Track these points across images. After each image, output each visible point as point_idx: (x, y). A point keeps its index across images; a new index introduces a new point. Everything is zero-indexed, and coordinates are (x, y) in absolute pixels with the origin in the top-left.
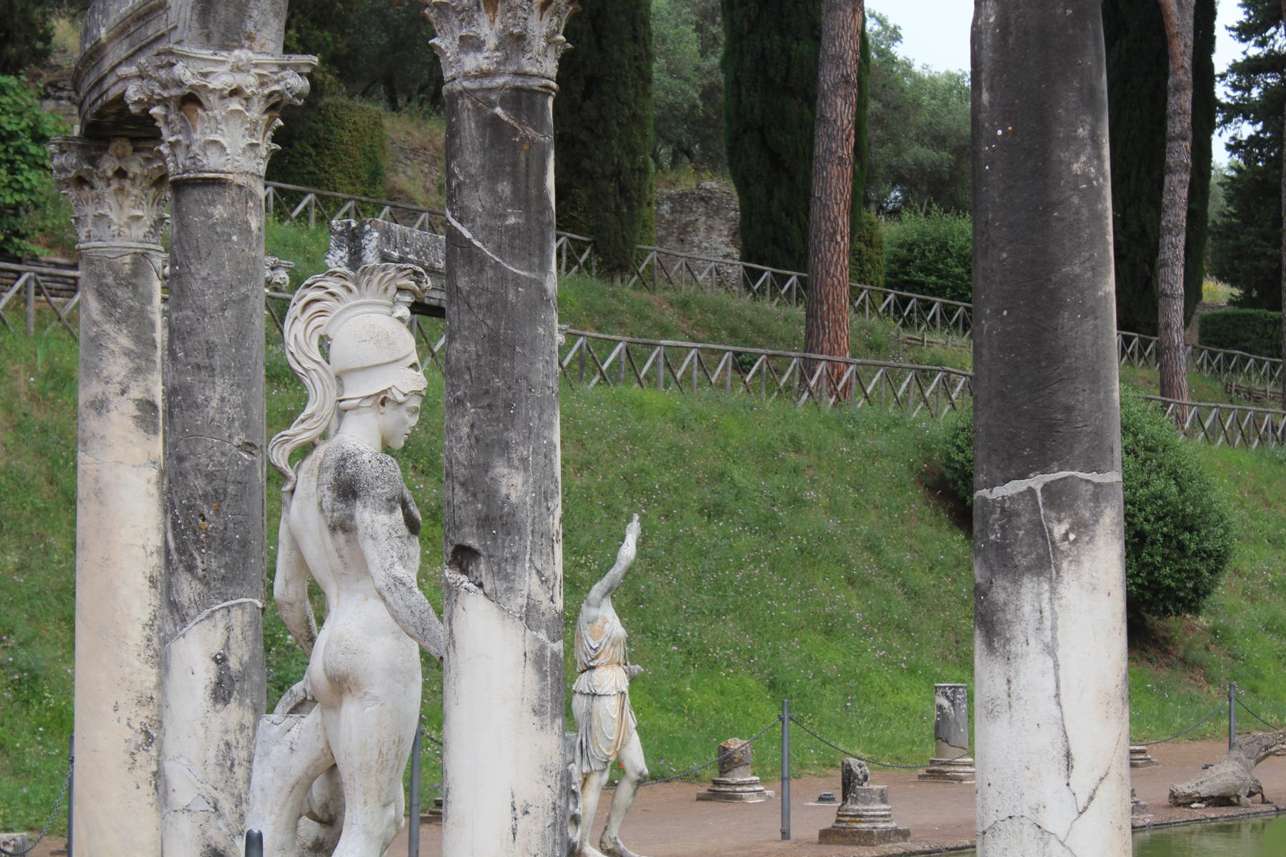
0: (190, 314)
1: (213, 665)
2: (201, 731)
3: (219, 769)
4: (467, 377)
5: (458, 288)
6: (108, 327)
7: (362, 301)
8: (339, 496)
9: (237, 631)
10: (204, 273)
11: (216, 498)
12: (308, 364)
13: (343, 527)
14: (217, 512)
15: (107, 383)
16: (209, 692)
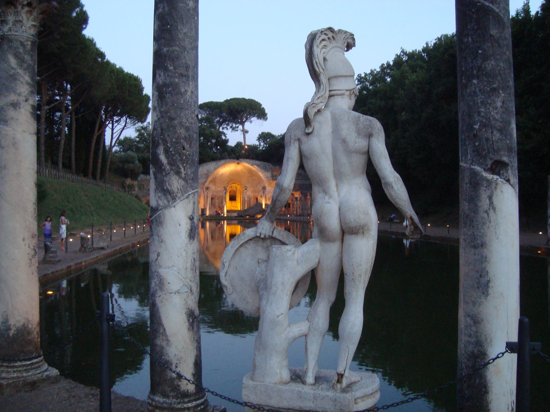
0: (177, 49)
1: (189, 221)
2: (184, 254)
4: (499, 78)
5: (491, 35)
6: (20, 71)
10: (185, 31)
14: (190, 146)
15: (19, 96)
16: (187, 234)
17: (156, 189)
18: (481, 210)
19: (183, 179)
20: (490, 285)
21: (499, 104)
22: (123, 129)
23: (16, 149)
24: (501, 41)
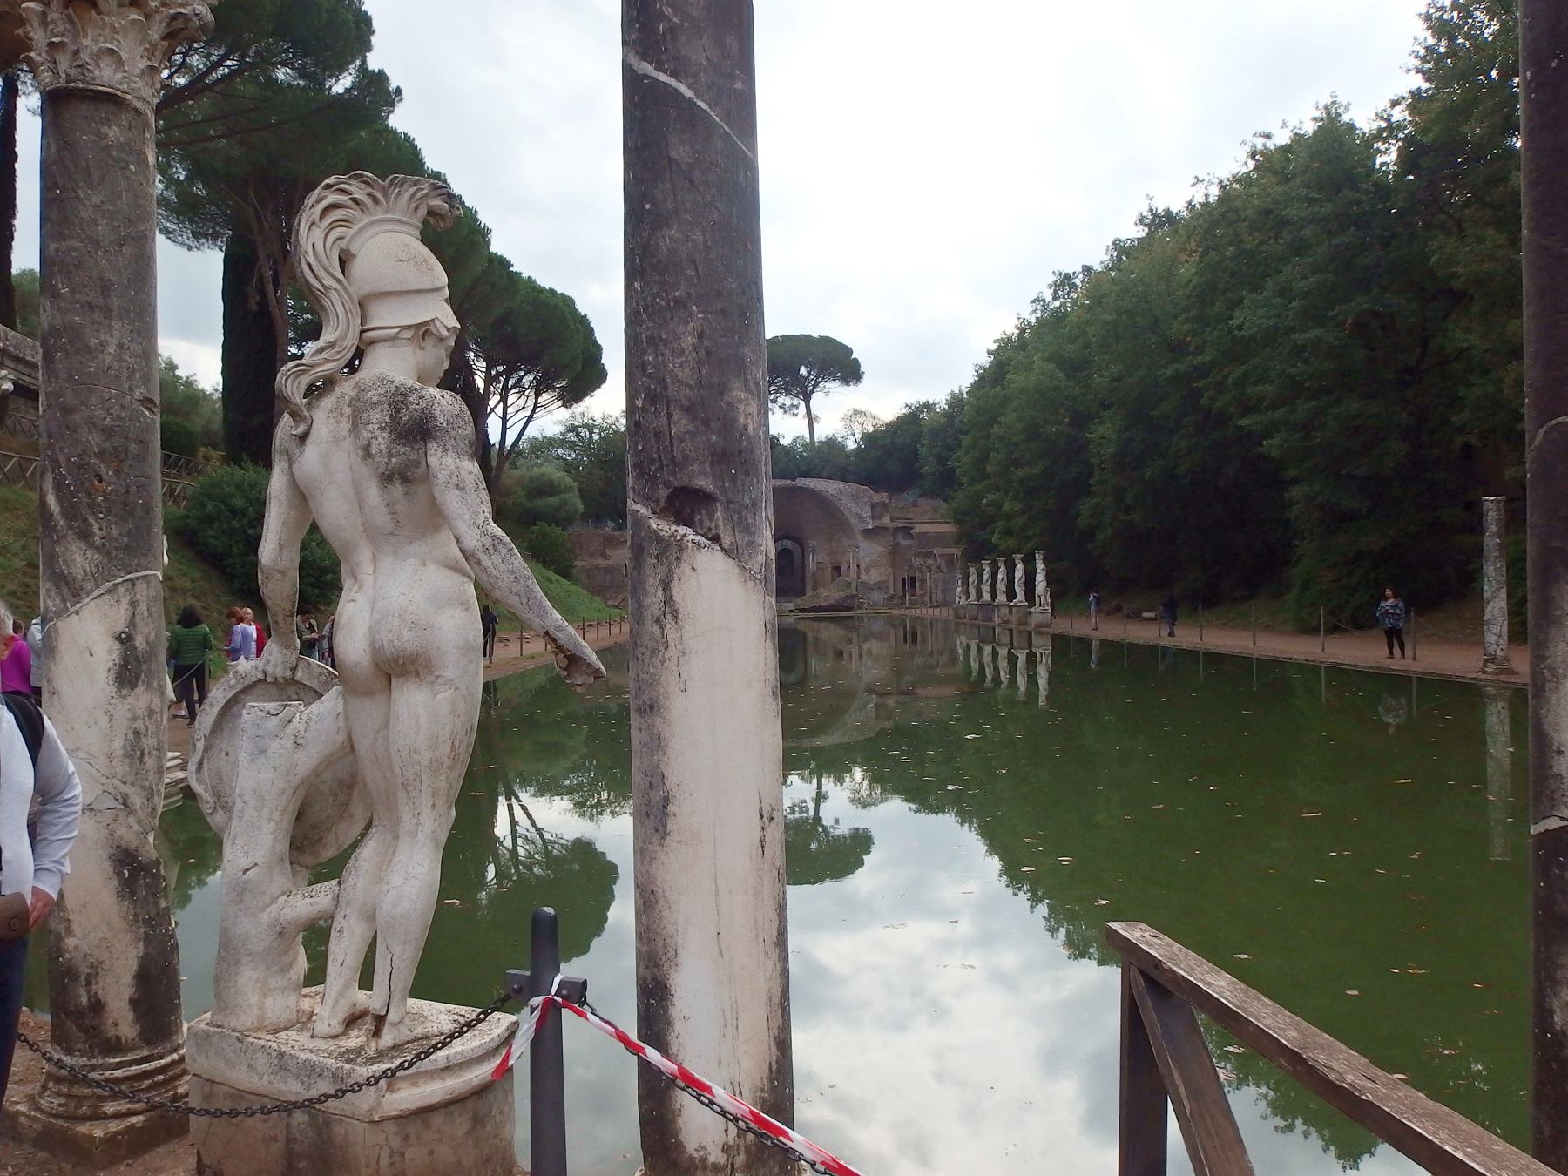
1: (117, 645)
2: (104, 720)
3: (127, 761)
4: (692, 273)
5: (671, 161)
7: (390, 216)
8: (399, 437)
9: (143, 606)
10: (96, 200)
11: (117, 457)
12: (329, 282)
13: (404, 476)
14: (117, 472)
16: (112, 674)
18: (648, 618)
19: (97, 548)
20: (671, 808)
21: (691, 340)
22: (530, 418)
24: (697, 174)
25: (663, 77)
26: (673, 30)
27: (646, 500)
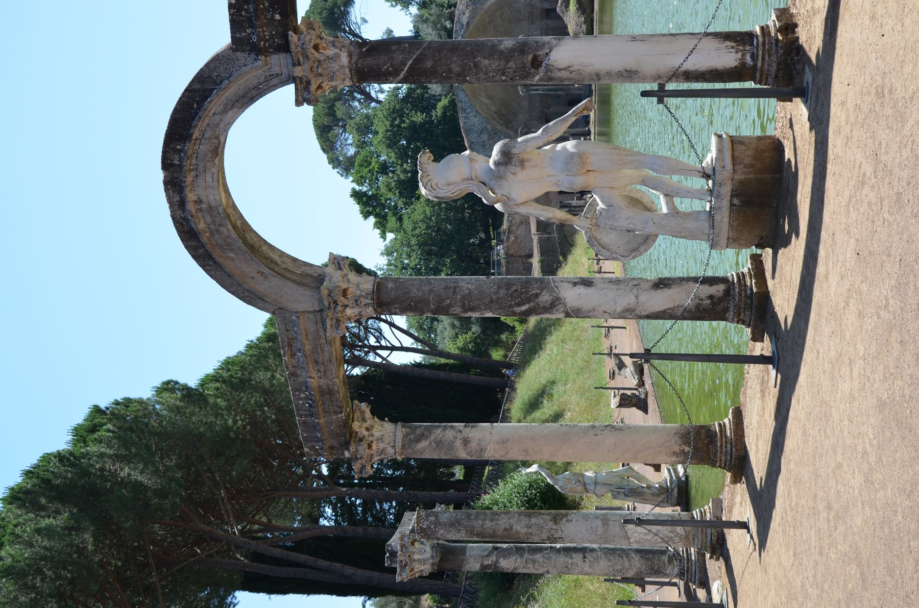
2: (604, 291)
6: (432, 438)
17: (550, 313)
18: (570, 76)
21: (486, 61)
23: (508, 440)
25: (406, 69)
26: (392, 66)
27: (534, 76)
